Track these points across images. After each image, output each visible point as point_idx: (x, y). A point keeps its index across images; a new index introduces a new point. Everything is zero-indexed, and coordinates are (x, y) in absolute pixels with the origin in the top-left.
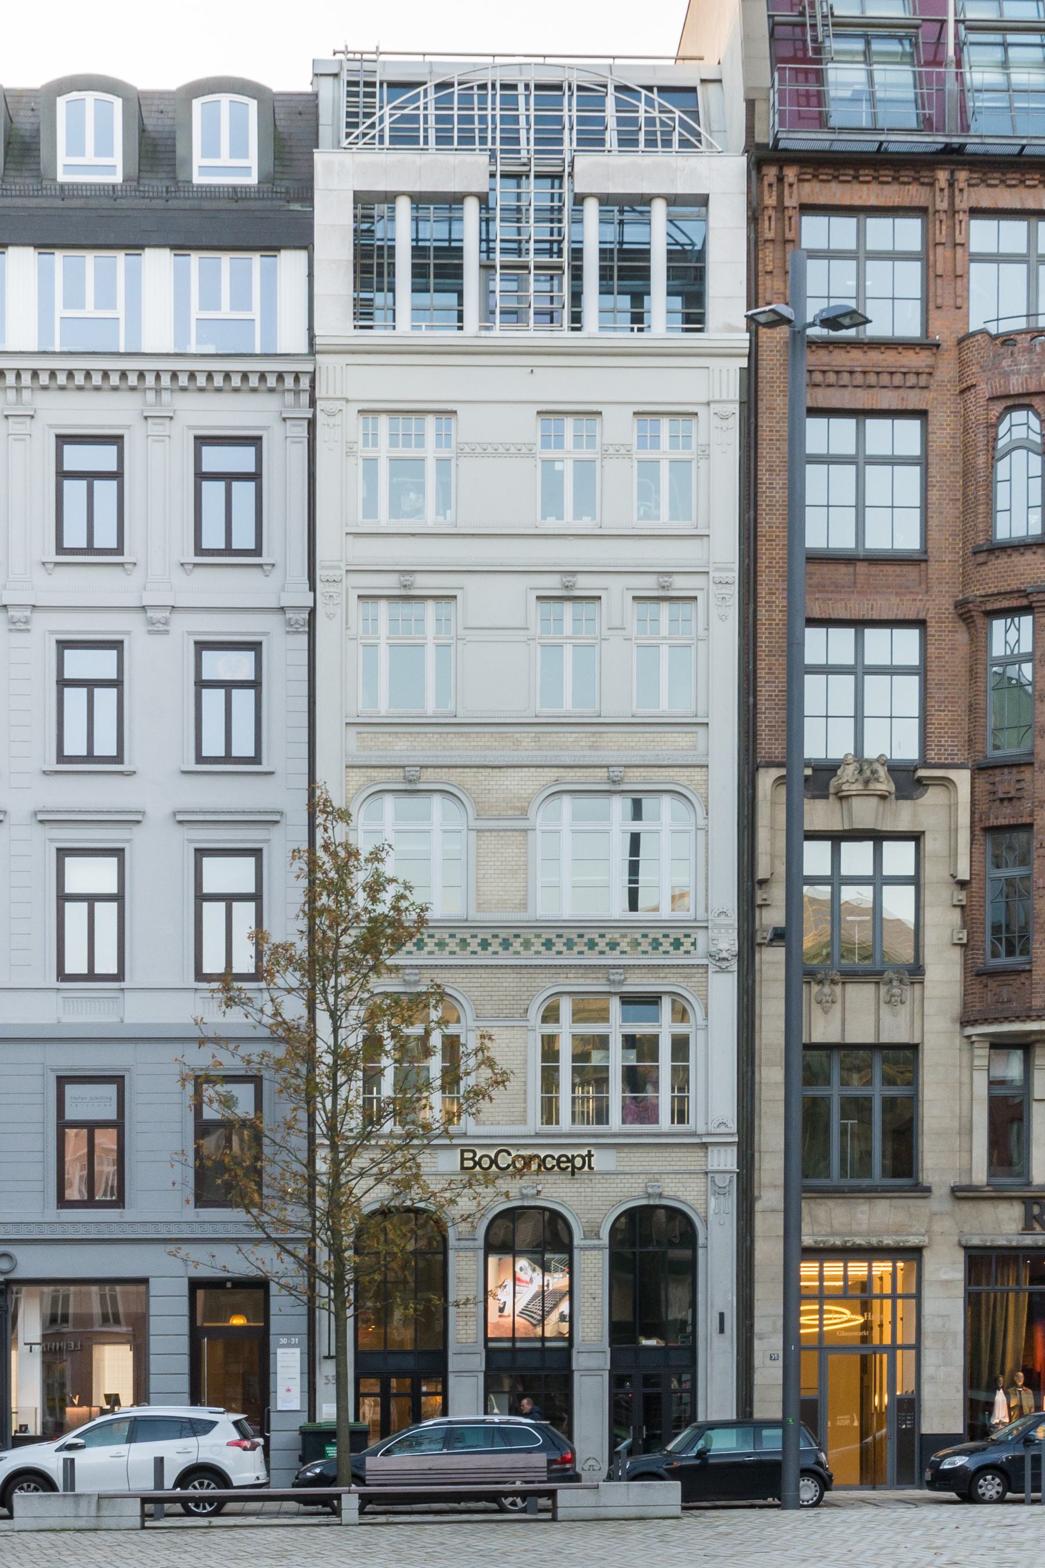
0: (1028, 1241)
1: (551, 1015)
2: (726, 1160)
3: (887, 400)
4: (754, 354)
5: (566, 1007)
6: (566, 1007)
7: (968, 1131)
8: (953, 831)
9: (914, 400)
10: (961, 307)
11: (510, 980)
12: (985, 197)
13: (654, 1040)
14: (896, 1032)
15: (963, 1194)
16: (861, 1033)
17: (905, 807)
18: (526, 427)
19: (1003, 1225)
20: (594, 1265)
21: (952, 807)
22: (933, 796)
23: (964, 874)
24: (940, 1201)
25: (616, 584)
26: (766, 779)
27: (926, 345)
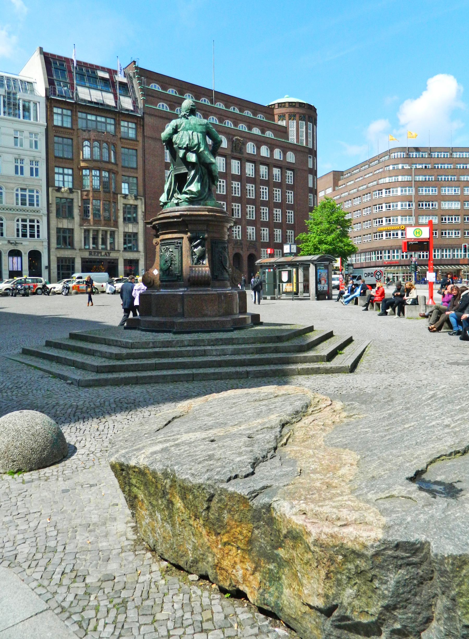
0: (90, 257)
1: (18, 221)
2: (46, 244)
3: (66, 136)
4: (47, 127)
5: (20, 220)
6: (20, 220)
7: (81, 241)
8: (78, 199)
9: (71, 137)
10: (77, 124)
11: (11, 215)
12: (80, 110)
13: (34, 226)
14: (70, 227)
15: (80, 250)
16: (65, 226)
17: (71, 195)
18: (13, 132)
19: (86, 255)
20: (26, 259)
21: (78, 195)
22: (75, 194)
23: (80, 205)
24: (78, 251)
25: (27, 157)
26: (50, 189)
27: (72, 129)
